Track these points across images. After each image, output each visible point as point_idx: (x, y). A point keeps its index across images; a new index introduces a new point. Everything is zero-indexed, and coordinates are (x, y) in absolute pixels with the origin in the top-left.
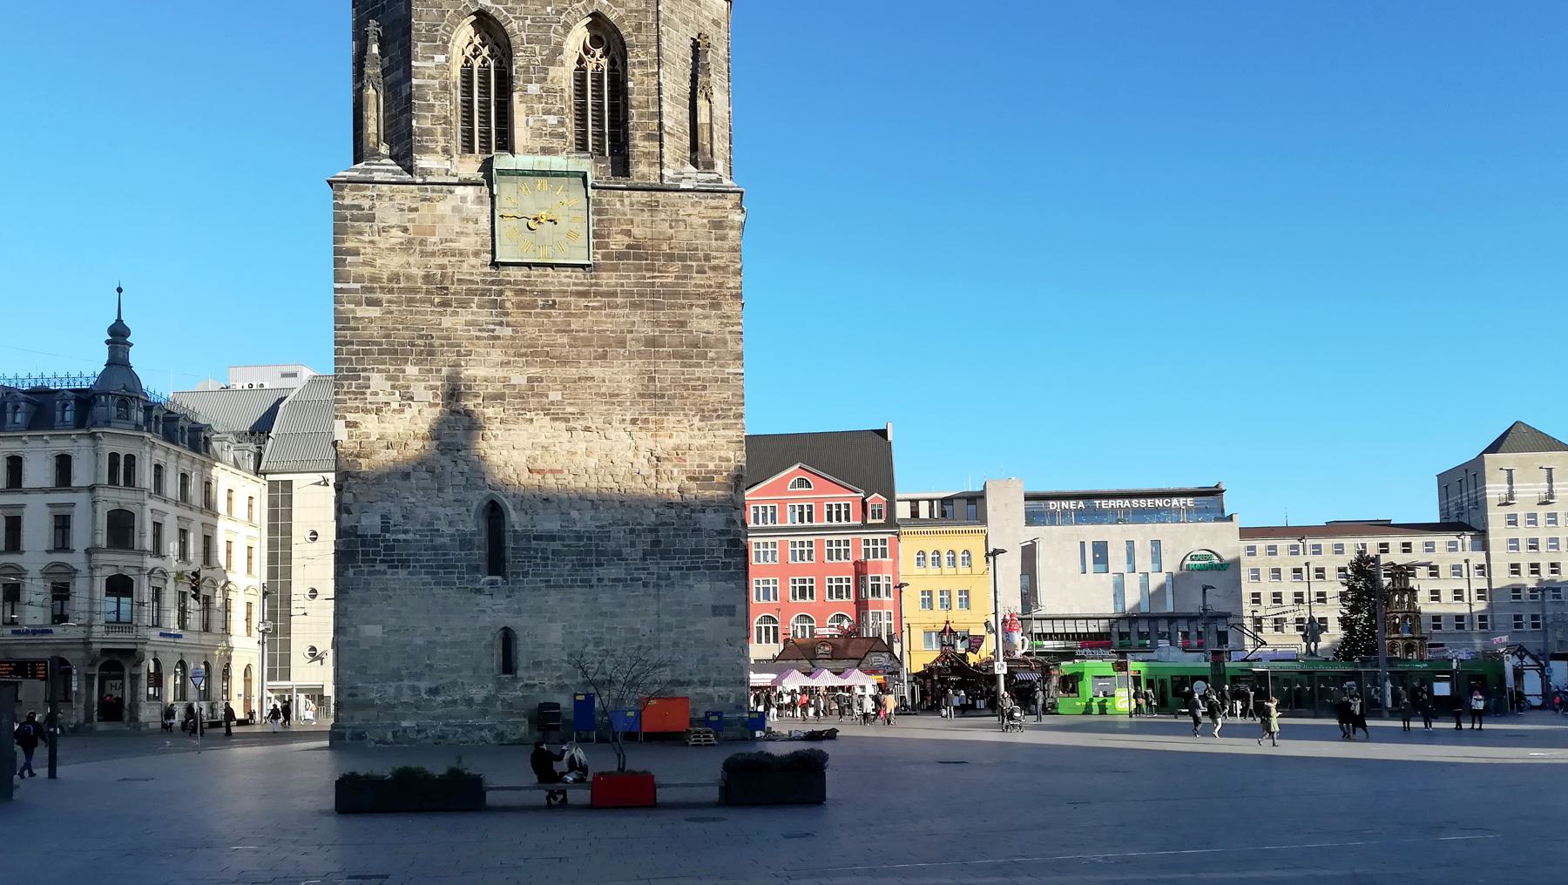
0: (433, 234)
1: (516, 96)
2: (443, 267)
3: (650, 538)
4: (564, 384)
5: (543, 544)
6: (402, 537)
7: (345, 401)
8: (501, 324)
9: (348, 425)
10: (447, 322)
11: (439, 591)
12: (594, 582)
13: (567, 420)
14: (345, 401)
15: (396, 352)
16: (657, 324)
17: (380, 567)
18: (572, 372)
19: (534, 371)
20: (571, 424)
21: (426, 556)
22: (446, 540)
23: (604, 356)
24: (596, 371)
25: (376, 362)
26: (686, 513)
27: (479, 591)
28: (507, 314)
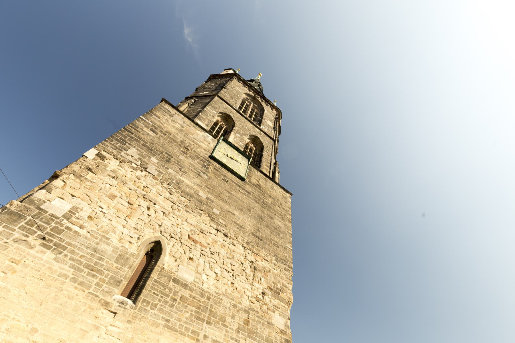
0: (192, 135)
1: (232, 133)
2: (190, 144)
3: (244, 316)
4: (222, 209)
5: (178, 287)
6: (76, 228)
7: (107, 146)
8: (204, 173)
9: (98, 155)
10: (182, 157)
11: (70, 287)
12: (201, 337)
13: (218, 224)
14: (107, 146)
15: (152, 150)
16: (263, 212)
17: (32, 239)
18: (227, 207)
19: (210, 196)
20: (220, 228)
21: (85, 252)
22: (109, 250)
23: (241, 210)
24: (236, 213)
25: (138, 145)
26: (265, 308)
27: (106, 304)
28: (208, 172)
